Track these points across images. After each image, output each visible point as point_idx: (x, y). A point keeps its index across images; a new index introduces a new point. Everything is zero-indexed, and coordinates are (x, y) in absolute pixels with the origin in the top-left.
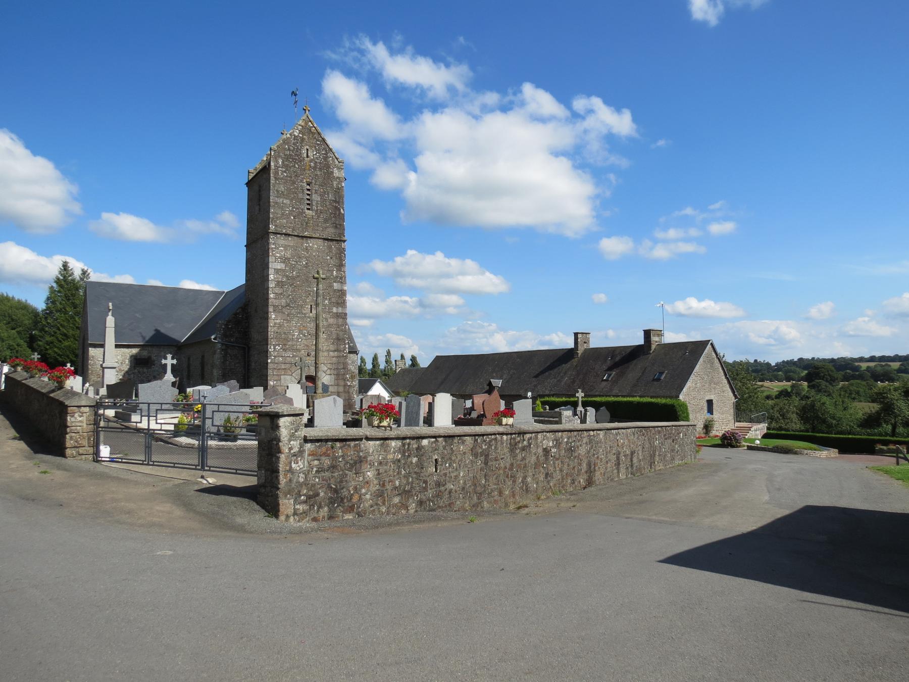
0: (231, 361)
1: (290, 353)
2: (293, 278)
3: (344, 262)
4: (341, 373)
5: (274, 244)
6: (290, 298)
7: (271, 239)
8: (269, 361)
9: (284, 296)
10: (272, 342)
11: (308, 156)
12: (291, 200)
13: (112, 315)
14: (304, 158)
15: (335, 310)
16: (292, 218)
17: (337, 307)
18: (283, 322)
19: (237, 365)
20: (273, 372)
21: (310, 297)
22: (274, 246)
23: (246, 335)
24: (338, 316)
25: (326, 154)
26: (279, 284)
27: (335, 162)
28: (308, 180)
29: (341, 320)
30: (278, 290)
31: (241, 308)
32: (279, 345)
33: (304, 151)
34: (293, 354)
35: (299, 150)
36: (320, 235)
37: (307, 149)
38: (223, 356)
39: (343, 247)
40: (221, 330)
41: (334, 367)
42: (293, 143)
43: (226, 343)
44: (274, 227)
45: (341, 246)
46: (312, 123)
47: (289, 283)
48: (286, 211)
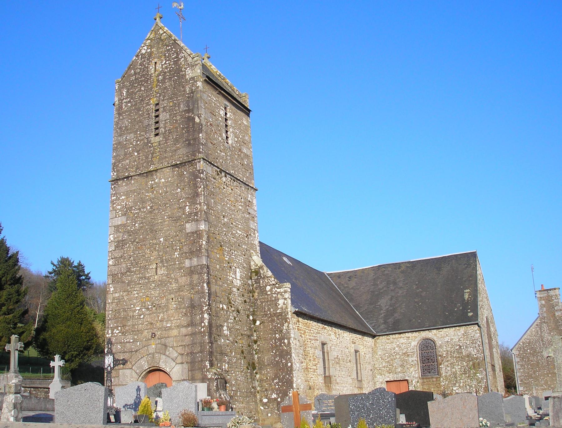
2: (136, 232)
9: (124, 259)
15: (187, 263)
16: (136, 154)
32: (117, 328)
34: (134, 339)
41: (188, 350)
44: (115, 174)
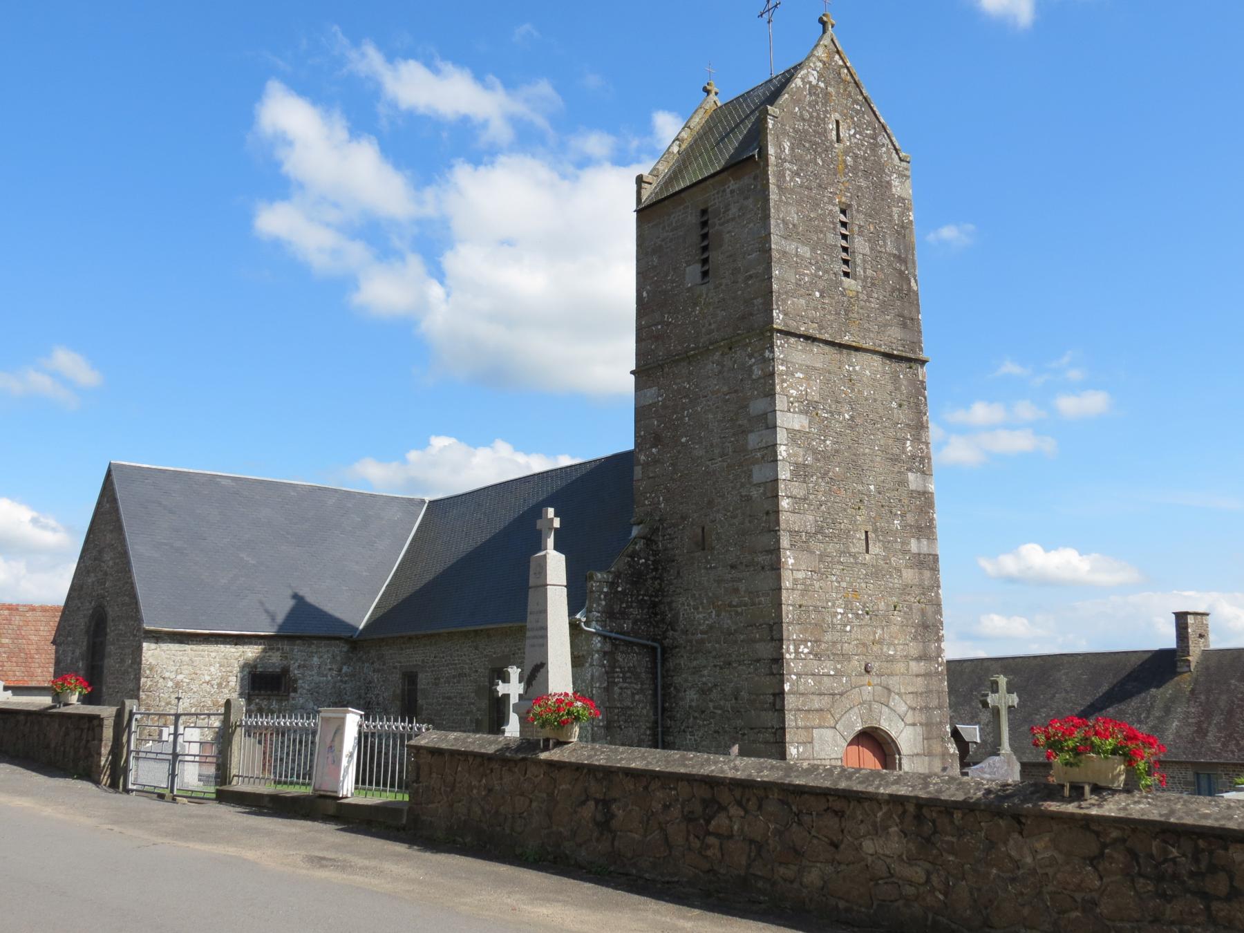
0: (625, 685)
1: (828, 663)
2: (825, 457)
3: (925, 418)
4: (934, 721)
5: (783, 362)
6: (824, 512)
7: (778, 347)
8: (787, 687)
9: (810, 505)
10: (791, 632)
11: (839, 140)
12: (813, 250)
13: (556, 548)
14: (832, 142)
15: (914, 546)
16: (817, 294)
17: (918, 539)
18: (812, 579)
19: (637, 697)
20: (796, 720)
21: (864, 511)
22: (784, 368)
23: (656, 614)
24: (921, 563)
25: (874, 137)
26: (801, 472)
27: (892, 159)
28: (843, 199)
29: (929, 572)
30: (798, 489)
31: (643, 538)
32: (805, 641)
33: (832, 126)
34: (835, 669)
35: (821, 121)
36: (874, 344)
37: (837, 122)
38: (607, 672)
39: (921, 378)
40: (600, 599)
41: (921, 702)
42: (810, 103)
43: (613, 635)
44: (781, 317)
45: (917, 375)
46: (841, 58)
47: (818, 469)
48: (804, 274)
